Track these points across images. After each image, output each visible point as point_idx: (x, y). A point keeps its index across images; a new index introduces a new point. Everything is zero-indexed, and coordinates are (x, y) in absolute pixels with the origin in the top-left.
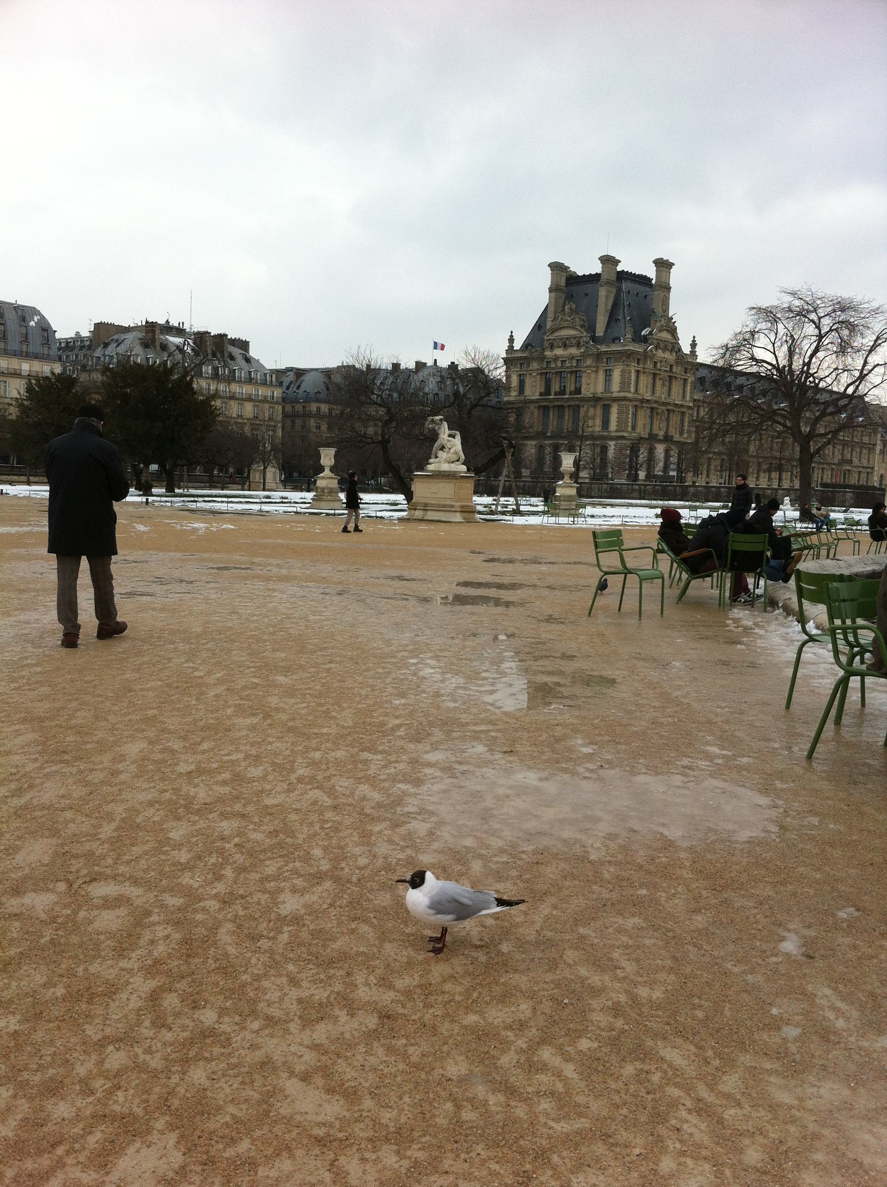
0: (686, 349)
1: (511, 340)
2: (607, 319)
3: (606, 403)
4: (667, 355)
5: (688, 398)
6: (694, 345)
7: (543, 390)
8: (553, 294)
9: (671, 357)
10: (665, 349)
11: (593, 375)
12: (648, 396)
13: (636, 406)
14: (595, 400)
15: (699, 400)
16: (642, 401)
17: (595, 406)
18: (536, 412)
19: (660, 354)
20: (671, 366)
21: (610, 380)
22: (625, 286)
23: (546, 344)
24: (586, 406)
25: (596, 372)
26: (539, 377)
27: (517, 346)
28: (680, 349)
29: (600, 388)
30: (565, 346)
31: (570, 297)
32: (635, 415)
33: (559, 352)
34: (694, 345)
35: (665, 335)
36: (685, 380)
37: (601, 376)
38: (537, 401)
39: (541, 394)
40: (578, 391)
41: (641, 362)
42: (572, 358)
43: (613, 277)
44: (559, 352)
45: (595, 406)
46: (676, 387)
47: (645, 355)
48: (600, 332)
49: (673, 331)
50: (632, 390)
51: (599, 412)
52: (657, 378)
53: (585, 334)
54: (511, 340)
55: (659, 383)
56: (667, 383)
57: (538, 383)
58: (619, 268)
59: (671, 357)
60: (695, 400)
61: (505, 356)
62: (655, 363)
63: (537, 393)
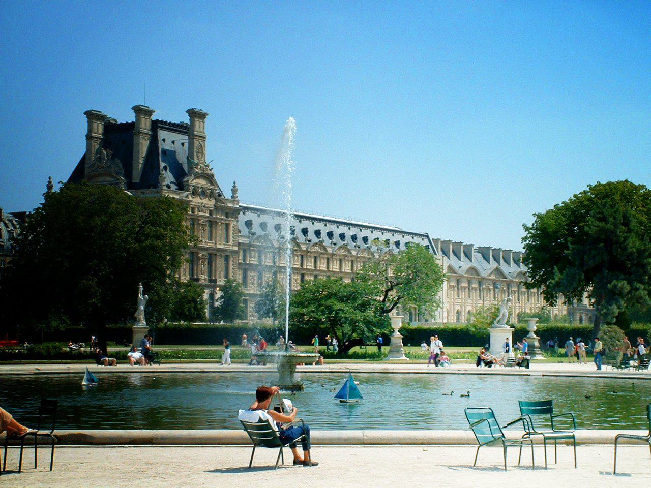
0: (227, 194)
1: (50, 186)
4: (205, 201)
5: (231, 243)
6: (234, 190)
9: (210, 203)
10: (204, 194)
20: (210, 211)
22: (162, 134)
34: (234, 190)
35: (202, 182)
48: (136, 179)
49: (210, 178)
54: (50, 186)
56: (207, 228)
58: (154, 118)
59: (210, 203)
60: (239, 244)
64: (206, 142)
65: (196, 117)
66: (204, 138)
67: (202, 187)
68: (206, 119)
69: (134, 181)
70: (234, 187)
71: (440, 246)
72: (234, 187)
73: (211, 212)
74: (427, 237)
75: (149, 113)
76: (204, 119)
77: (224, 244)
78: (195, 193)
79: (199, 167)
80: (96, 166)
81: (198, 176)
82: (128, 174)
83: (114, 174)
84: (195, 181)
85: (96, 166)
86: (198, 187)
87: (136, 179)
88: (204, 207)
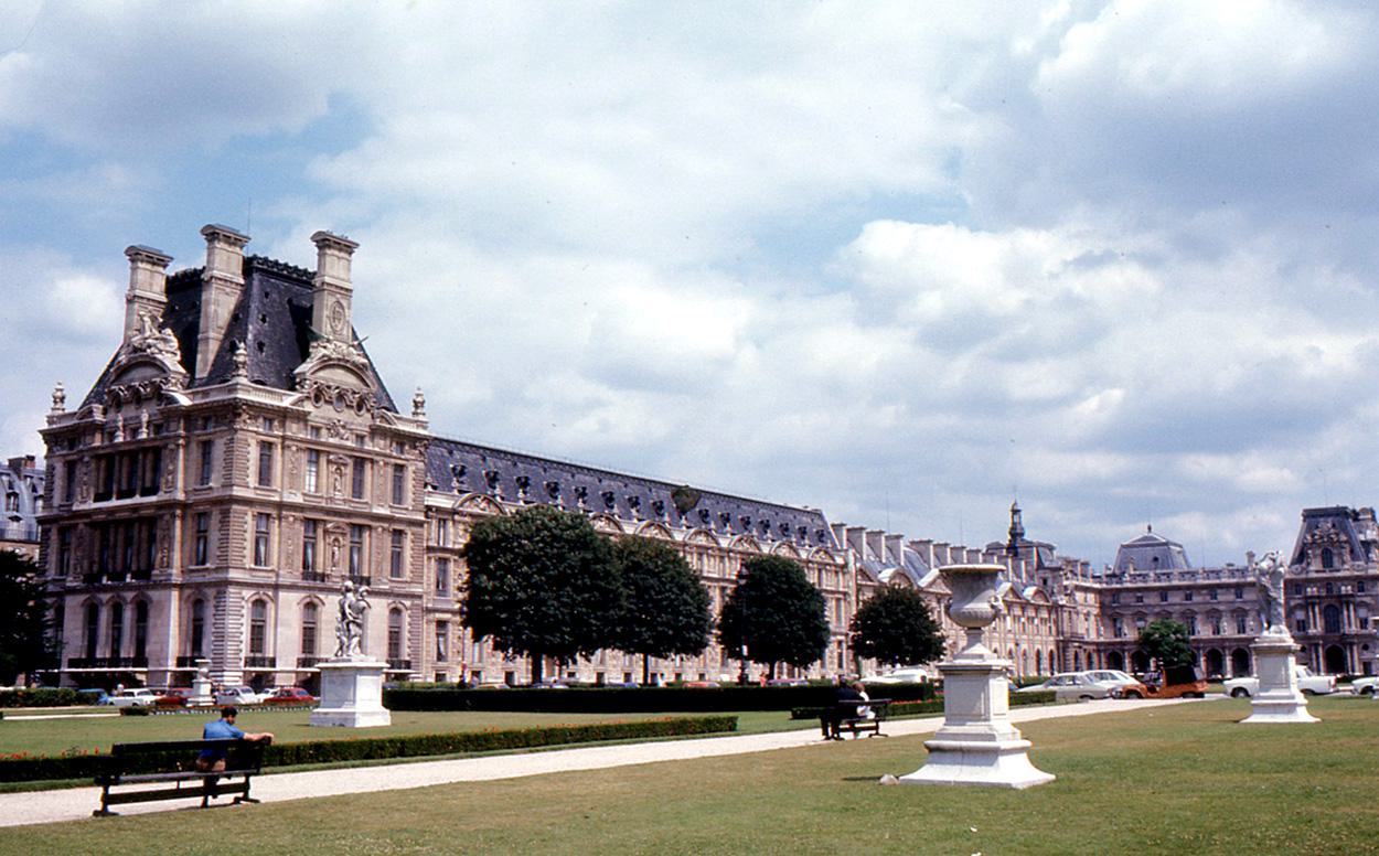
0: (405, 410)
4: (347, 416)
9: (363, 421)
13: (268, 516)
15: (439, 510)
16: (281, 506)
19: (319, 413)
36: (400, 468)
46: (376, 480)
47: (283, 415)
48: (202, 371)
49: (361, 371)
50: (253, 480)
56: (349, 471)
58: (248, 252)
59: (359, 420)
60: (429, 508)
61: (46, 426)
64: (353, 300)
65: (330, 247)
66: (351, 291)
67: (337, 388)
68: (353, 255)
71: (845, 538)
74: (820, 516)
75: (236, 240)
76: (350, 254)
77: (391, 507)
78: (318, 396)
81: (327, 363)
84: (321, 374)
86: (329, 387)
87: (202, 371)
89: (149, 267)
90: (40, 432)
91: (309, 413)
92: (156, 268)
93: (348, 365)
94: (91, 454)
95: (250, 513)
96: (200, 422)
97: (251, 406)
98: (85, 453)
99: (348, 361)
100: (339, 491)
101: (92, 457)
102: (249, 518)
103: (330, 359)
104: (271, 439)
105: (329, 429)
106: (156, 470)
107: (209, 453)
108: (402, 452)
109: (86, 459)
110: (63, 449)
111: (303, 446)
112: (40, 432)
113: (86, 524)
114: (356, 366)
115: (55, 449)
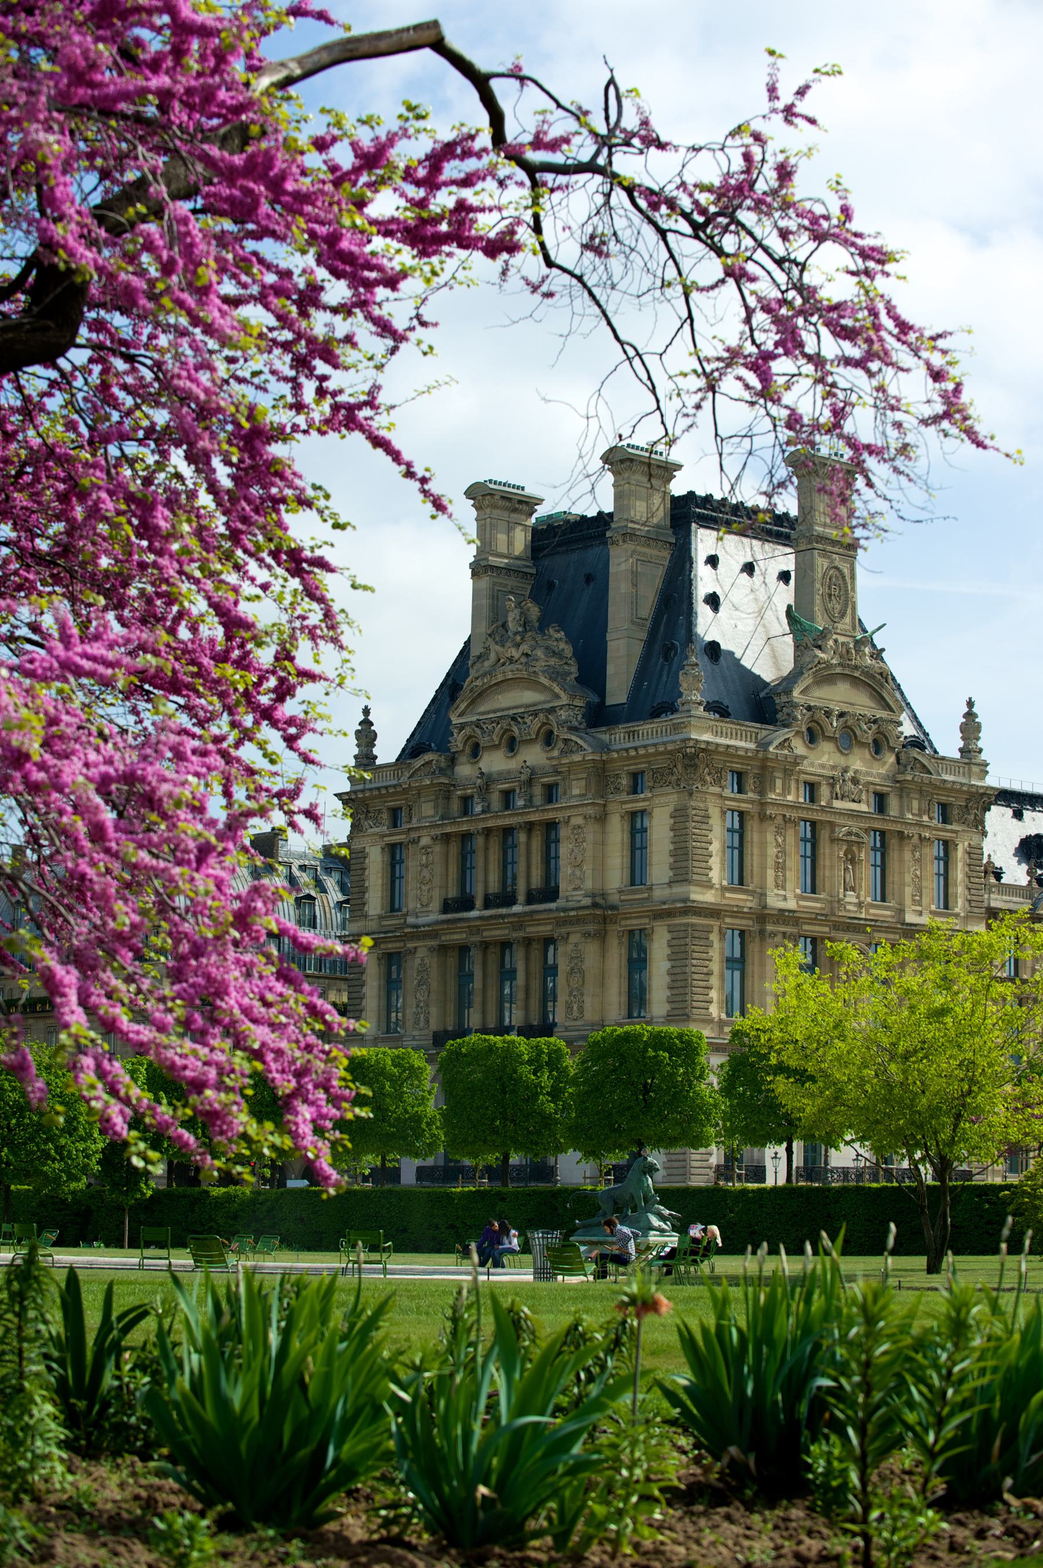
0: (947, 743)
1: (366, 735)
2: (638, 649)
3: (635, 923)
5: (960, 906)
6: (970, 727)
7: (453, 893)
8: (485, 582)
10: (848, 738)
11: (590, 833)
12: (786, 897)
14: (601, 914)
17: (601, 937)
18: (433, 963)
19: (823, 759)
21: (643, 848)
23: (457, 741)
24: (574, 939)
25: (602, 819)
26: (438, 848)
27: (388, 750)
28: (920, 743)
29: (616, 877)
30: (512, 745)
31: (542, 588)
32: (738, 963)
33: (495, 762)
34: (970, 727)
37: (617, 832)
38: (431, 933)
39: (447, 907)
40: (549, 892)
41: (750, 783)
42: (530, 782)
43: (660, 513)
44: (495, 762)
45: (601, 937)
49: (880, 684)
51: (616, 957)
52: (824, 835)
53: (565, 699)
54: (366, 735)
55: (831, 855)
57: (438, 869)
58: (678, 487)
61: (346, 787)
62: (812, 789)
63: (436, 905)
67: (842, 715)
69: (609, 701)
70: (970, 715)
72: (970, 715)
73: (881, 801)
79: (831, 643)
80: (493, 656)
82: (591, 672)
83: (543, 680)
85: (493, 656)
86: (828, 714)
88: (855, 781)
89: (506, 514)
90: (339, 796)
91: (805, 758)
92: (515, 516)
93: (857, 674)
94: (438, 832)
95: (716, 929)
96: (625, 781)
97: (708, 750)
98: (424, 832)
99: (856, 668)
100: (853, 889)
101: (434, 839)
102: (714, 937)
103: (829, 666)
104: (744, 806)
105: (832, 786)
106: (550, 859)
107: (644, 830)
108: (945, 821)
109: (425, 841)
110: (378, 823)
111: (794, 815)
112: (339, 796)
113: (431, 949)
114: (867, 674)
115: (366, 824)
